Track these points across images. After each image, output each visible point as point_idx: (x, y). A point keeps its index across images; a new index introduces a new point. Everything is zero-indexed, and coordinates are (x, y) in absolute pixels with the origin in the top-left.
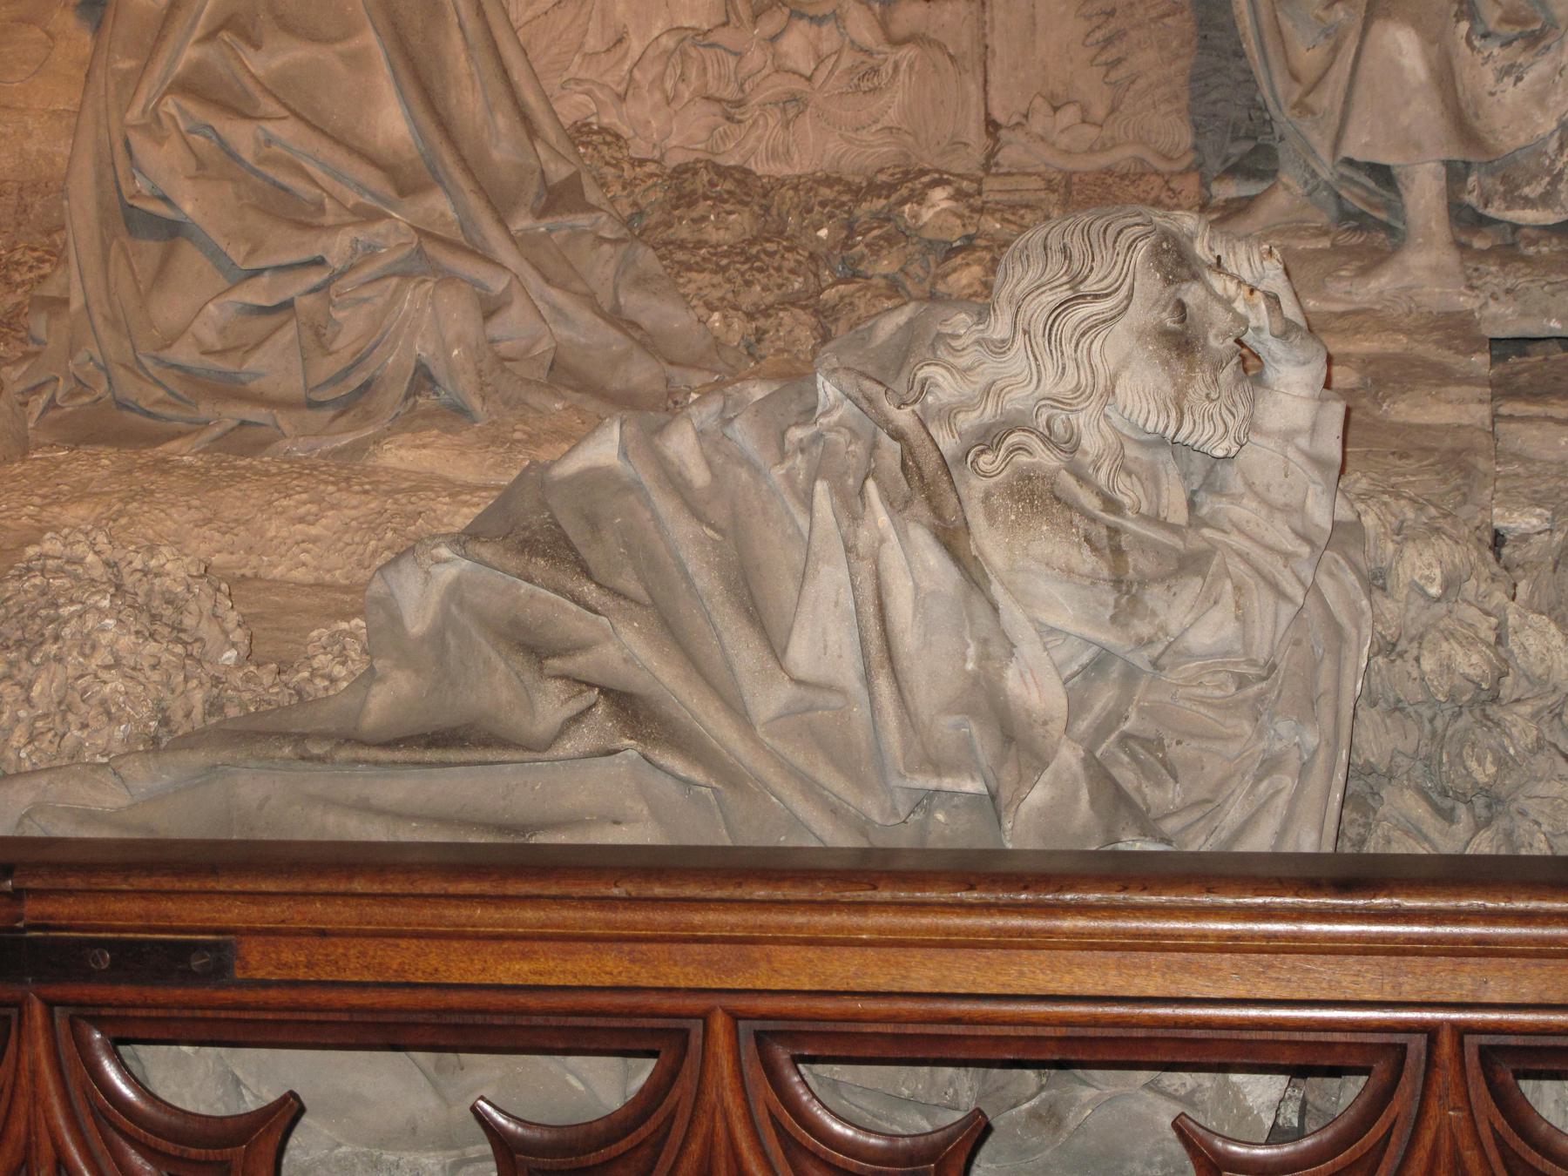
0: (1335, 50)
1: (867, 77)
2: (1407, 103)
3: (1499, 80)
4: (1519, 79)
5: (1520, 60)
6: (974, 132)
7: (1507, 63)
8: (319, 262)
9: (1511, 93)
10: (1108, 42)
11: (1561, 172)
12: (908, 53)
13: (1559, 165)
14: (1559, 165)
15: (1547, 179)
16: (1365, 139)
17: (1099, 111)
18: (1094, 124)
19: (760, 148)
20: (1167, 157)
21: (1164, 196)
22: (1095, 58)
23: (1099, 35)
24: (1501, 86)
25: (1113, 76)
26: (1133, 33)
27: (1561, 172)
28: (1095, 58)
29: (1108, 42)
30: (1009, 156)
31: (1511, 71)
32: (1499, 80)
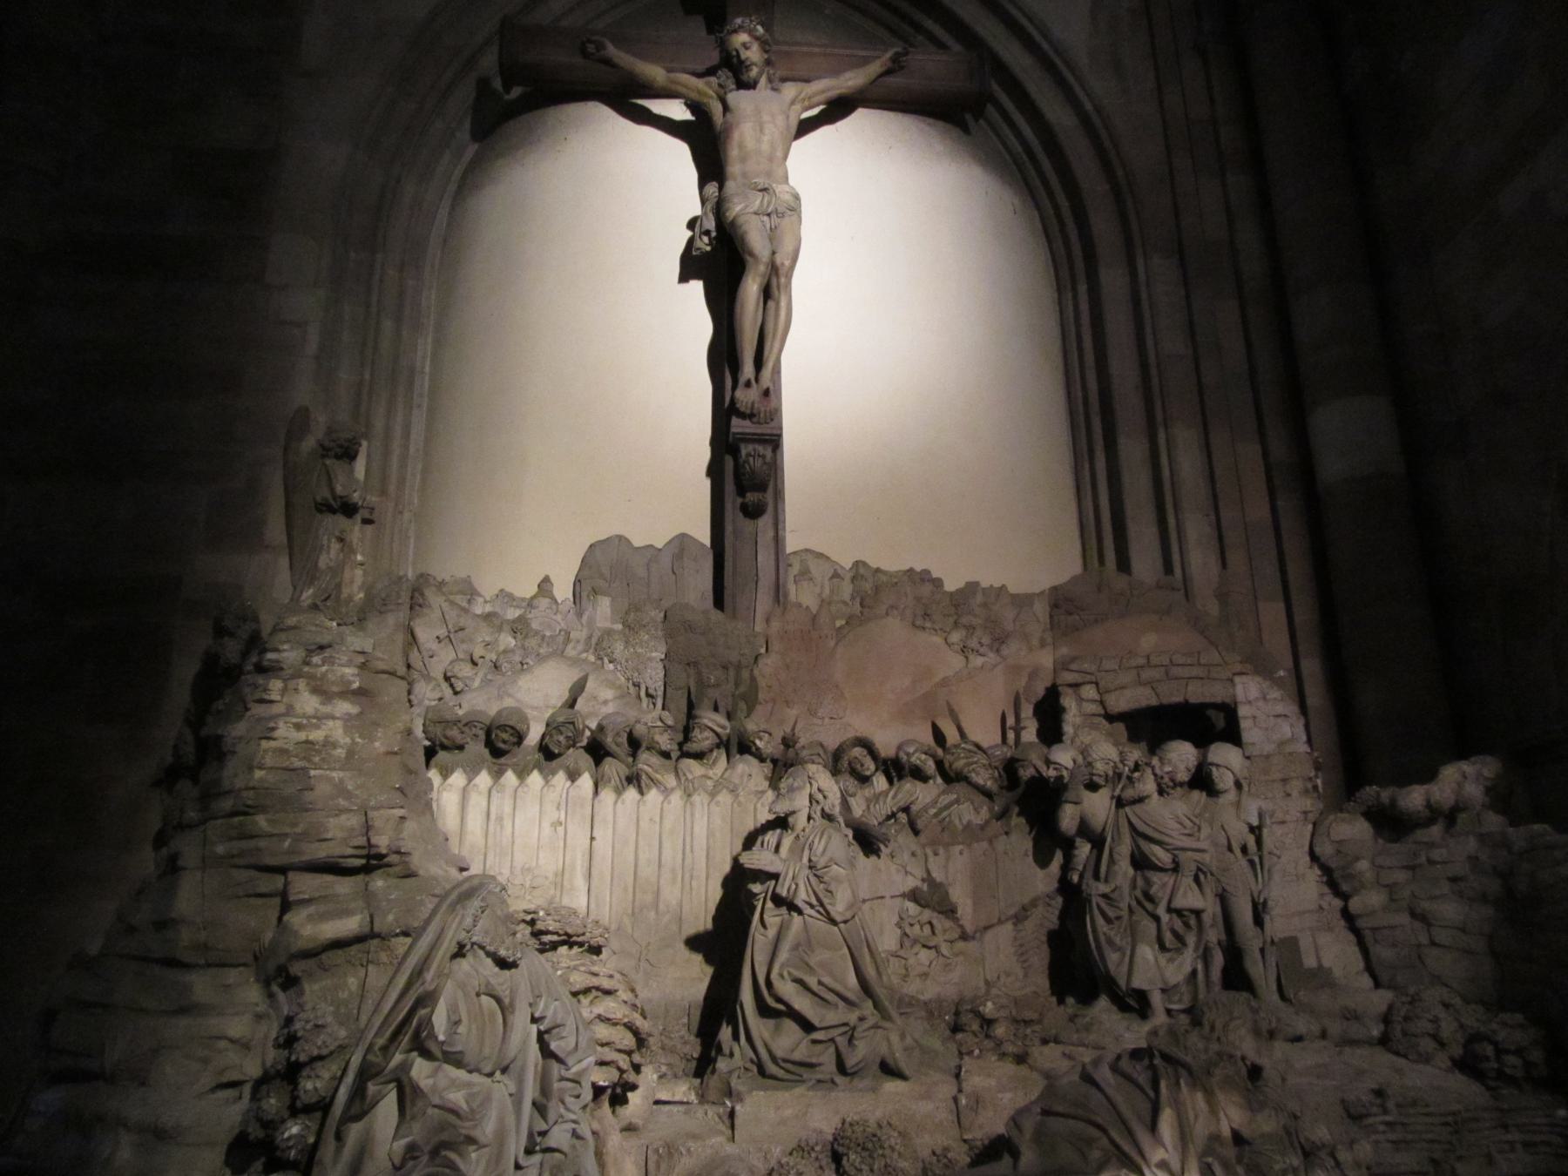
0: (1124, 955)
1: (947, 967)
6: (982, 984)
8: (845, 1024)
12: (961, 958)
19: (912, 988)
30: (994, 991)
31: (1171, 960)
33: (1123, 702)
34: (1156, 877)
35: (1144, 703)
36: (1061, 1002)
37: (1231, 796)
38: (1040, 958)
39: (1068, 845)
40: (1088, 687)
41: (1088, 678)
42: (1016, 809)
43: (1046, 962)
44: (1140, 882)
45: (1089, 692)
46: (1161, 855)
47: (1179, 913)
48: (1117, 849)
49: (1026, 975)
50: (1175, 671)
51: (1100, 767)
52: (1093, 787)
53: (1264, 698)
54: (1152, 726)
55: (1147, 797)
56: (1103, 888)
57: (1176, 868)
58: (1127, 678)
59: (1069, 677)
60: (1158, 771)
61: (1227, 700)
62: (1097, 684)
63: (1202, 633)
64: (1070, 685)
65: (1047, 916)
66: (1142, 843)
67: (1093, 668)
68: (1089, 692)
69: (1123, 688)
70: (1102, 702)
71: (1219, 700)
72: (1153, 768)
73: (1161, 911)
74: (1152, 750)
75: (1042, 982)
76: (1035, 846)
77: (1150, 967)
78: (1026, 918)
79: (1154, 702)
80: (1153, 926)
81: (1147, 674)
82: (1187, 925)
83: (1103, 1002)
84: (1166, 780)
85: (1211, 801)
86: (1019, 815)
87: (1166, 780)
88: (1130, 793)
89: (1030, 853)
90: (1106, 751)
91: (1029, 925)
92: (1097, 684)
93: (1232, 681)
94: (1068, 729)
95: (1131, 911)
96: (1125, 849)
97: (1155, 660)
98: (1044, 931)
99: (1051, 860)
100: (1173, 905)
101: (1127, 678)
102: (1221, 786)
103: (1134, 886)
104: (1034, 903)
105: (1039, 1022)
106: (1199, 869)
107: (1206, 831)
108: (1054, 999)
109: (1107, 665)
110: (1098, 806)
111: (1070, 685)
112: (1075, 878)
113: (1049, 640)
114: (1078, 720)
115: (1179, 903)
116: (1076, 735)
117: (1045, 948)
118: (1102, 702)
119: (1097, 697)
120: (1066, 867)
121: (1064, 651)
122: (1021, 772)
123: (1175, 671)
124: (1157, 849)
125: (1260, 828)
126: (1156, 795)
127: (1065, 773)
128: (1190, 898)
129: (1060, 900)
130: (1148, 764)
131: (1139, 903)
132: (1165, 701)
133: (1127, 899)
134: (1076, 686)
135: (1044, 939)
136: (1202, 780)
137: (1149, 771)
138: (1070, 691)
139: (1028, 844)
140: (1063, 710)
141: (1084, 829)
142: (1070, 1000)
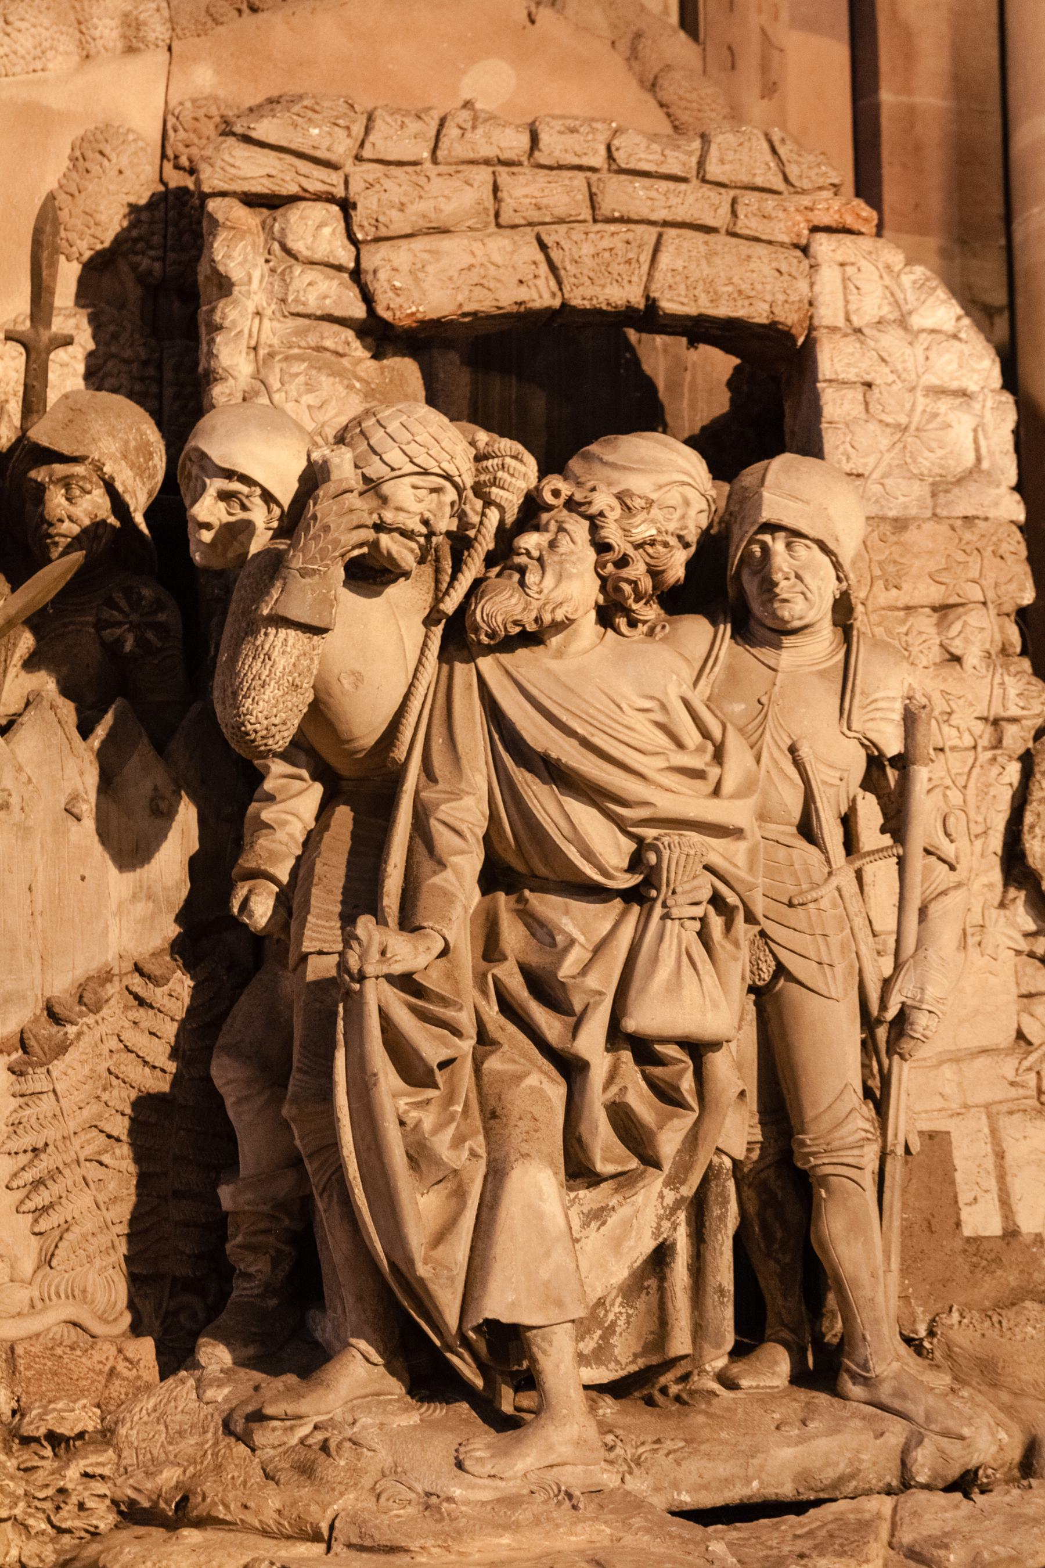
2: (548, 1254)
3: (585, 1225)
4: (604, 1223)
5: (613, 1202)
7: (595, 1206)
9: (594, 1239)
10: (39, 1183)
11: (613, 1324)
13: (611, 1317)
14: (611, 1317)
15: (599, 1332)
16: (511, 1297)
17: (27, 1266)
18: (22, 1281)
20: (102, 1319)
21: (121, 1366)
22: (22, 1202)
23: (28, 1176)
24: (585, 1232)
25: (43, 1225)
26: (66, 1172)
27: (613, 1324)
28: (22, 1202)
29: (39, 1183)
32: (585, 1225)
33: (428, 285)
34: (577, 922)
35: (506, 296)
36: (176, 1357)
37: (820, 645)
38: (103, 1197)
39: (230, 786)
40: (320, 211)
41: (318, 179)
42: (26, 641)
43: (123, 1211)
44: (513, 936)
45: (316, 230)
46: (602, 846)
47: (643, 1050)
48: (446, 811)
49: (47, 1261)
50: (623, 196)
51: (411, 502)
52: (369, 573)
53: (902, 322)
54: (549, 377)
55: (558, 627)
56: (408, 954)
57: (643, 892)
58: (461, 196)
59: (255, 170)
60: (612, 533)
61: (789, 317)
62: (346, 206)
63: (653, 86)
64: (252, 201)
65: (136, 1047)
66: (543, 800)
67: (341, 148)
68: (316, 230)
69: (444, 231)
70: (356, 275)
71: (759, 314)
72: (595, 523)
73: (591, 1043)
74: (551, 464)
75: (107, 1287)
76: (107, 783)
77: (565, 1256)
78: (62, 1048)
79: (542, 295)
80: (556, 1091)
81: (523, 191)
82: (667, 1095)
83: (359, 1372)
84: (637, 570)
85: (746, 657)
86: (30, 664)
87: (637, 570)
88: (503, 607)
89: (87, 808)
90: (433, 455)
91: (70, 1072)
92: (346, 206)
93: (805, 250)
94: (232, 358)
95: (484, 1038)
96: (466, 811)
97: (554, 144)
98: (122, 1098)
99: (161, 836)
100: (631, 1024)
101: (461, 196)
102: (794, 609)
103: (491, 949)
104: (88, 996)
105: (106, 1436)
106: (716, 900)
107: (738, 760)
108: (145, 1349)
109: (393, 139)
110: (368, 653)
111: (252, 201)
112: (262, 909)
113: (157, 30)
114: (274, 331)
115: (646, 1017)
116: (257, 376)
117: (122, 1160)
118: (356, 275)
119: (345, 256)
120: (216, 869)
121: (202, 78)
122: (56, 500)
123: (623, 196)
124: (587, 818)
125: (903, 762)
126: (588, 623)
127: (259, 515)
128: (698, 999)
129: (181, 986)
130: (571, 505)
131: (508, 1008)
132: (577, 302)
133: (470, 994)
134: (269, 202)
135: (120, 1126)
136: (722, 585)
137: (579, 528)
138: (240, 213)
139: (83, 776)
140: (224, 286)
141: (318, 742)
142: (215, 1355)
